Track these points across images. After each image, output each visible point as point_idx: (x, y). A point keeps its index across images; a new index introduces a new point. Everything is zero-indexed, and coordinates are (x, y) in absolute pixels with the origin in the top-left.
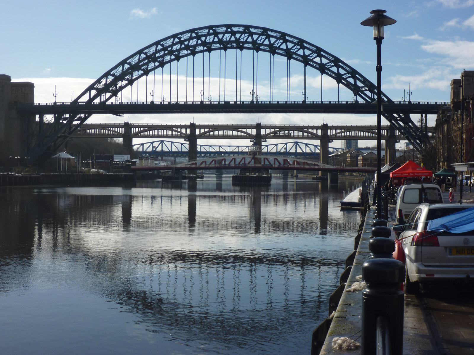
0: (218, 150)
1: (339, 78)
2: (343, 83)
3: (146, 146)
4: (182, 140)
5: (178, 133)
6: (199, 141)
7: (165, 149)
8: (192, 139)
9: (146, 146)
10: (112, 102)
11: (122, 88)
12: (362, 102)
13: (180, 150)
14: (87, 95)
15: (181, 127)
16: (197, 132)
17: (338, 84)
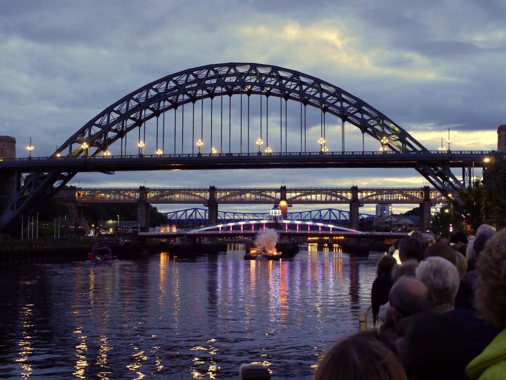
0: (232, 218)
1: (364, 127)
2: (369, 132)
3: (179, 214)
4: (201, 206)
6: (221, 208)
7: (198, 217)
8: (212, 205)
9: (179, 214)
11: (111, 141)
12: (391, 153)
13: (223, 218)
14: (68, 148)
15: (200, 190)
16: (218, 195)
17: (363, 133)
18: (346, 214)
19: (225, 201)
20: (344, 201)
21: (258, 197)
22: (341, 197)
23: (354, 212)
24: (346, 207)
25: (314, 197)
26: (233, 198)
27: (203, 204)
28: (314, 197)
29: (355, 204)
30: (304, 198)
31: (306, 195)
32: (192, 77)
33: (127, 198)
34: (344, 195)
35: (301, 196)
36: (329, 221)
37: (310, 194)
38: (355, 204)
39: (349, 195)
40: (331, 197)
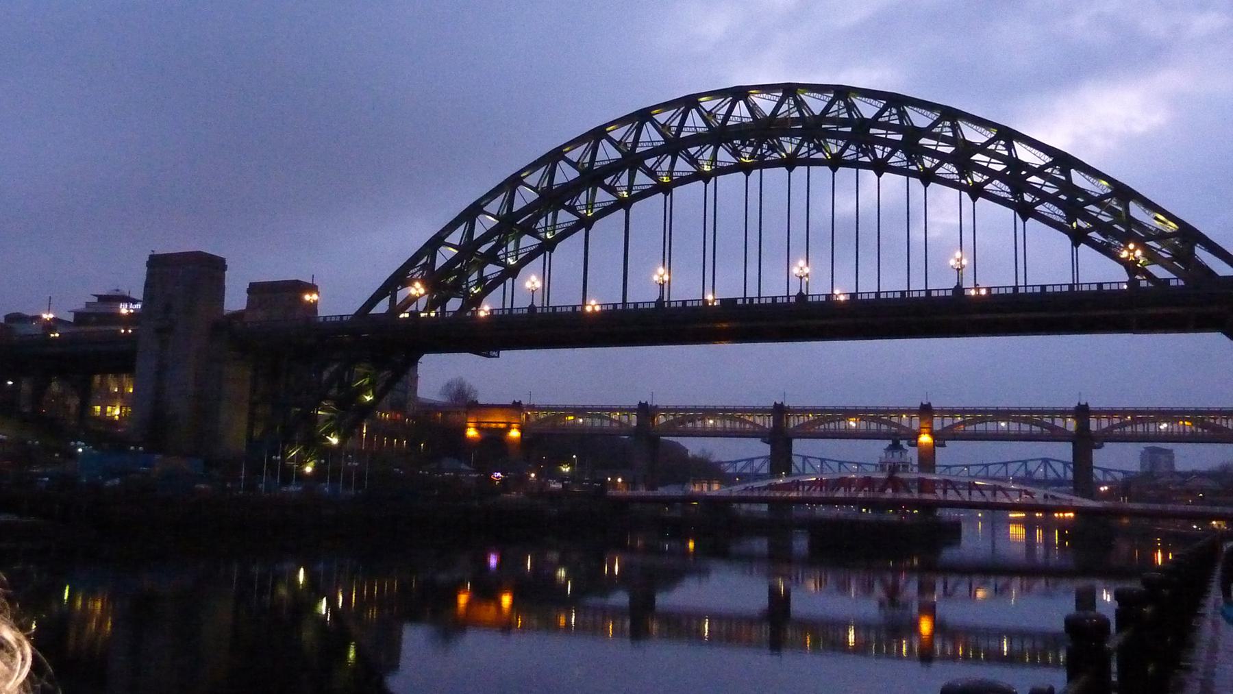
5: (748, 426)
10: (342, 314)
18: (1059, 468)
19: (806, 433)
20: (1056, 435)
21: (874, 426)
22: (1052, 428)
23: (1082, 462)
24: (1065, 451)
25: (991, 426)
26: (832, 426)
27: (760, 439)
28: (991, 426)
29: (1084, 442)
30: (970, 428)
31: (975, 421)
32: (741, 110)
33: (614, 425)
34: (1059, 422)
35: (964, 423)
36: (1044, 483)
37: (983, 420)
38: (1084, 442)
39: (1071, 424)
40: (1031, 428)
